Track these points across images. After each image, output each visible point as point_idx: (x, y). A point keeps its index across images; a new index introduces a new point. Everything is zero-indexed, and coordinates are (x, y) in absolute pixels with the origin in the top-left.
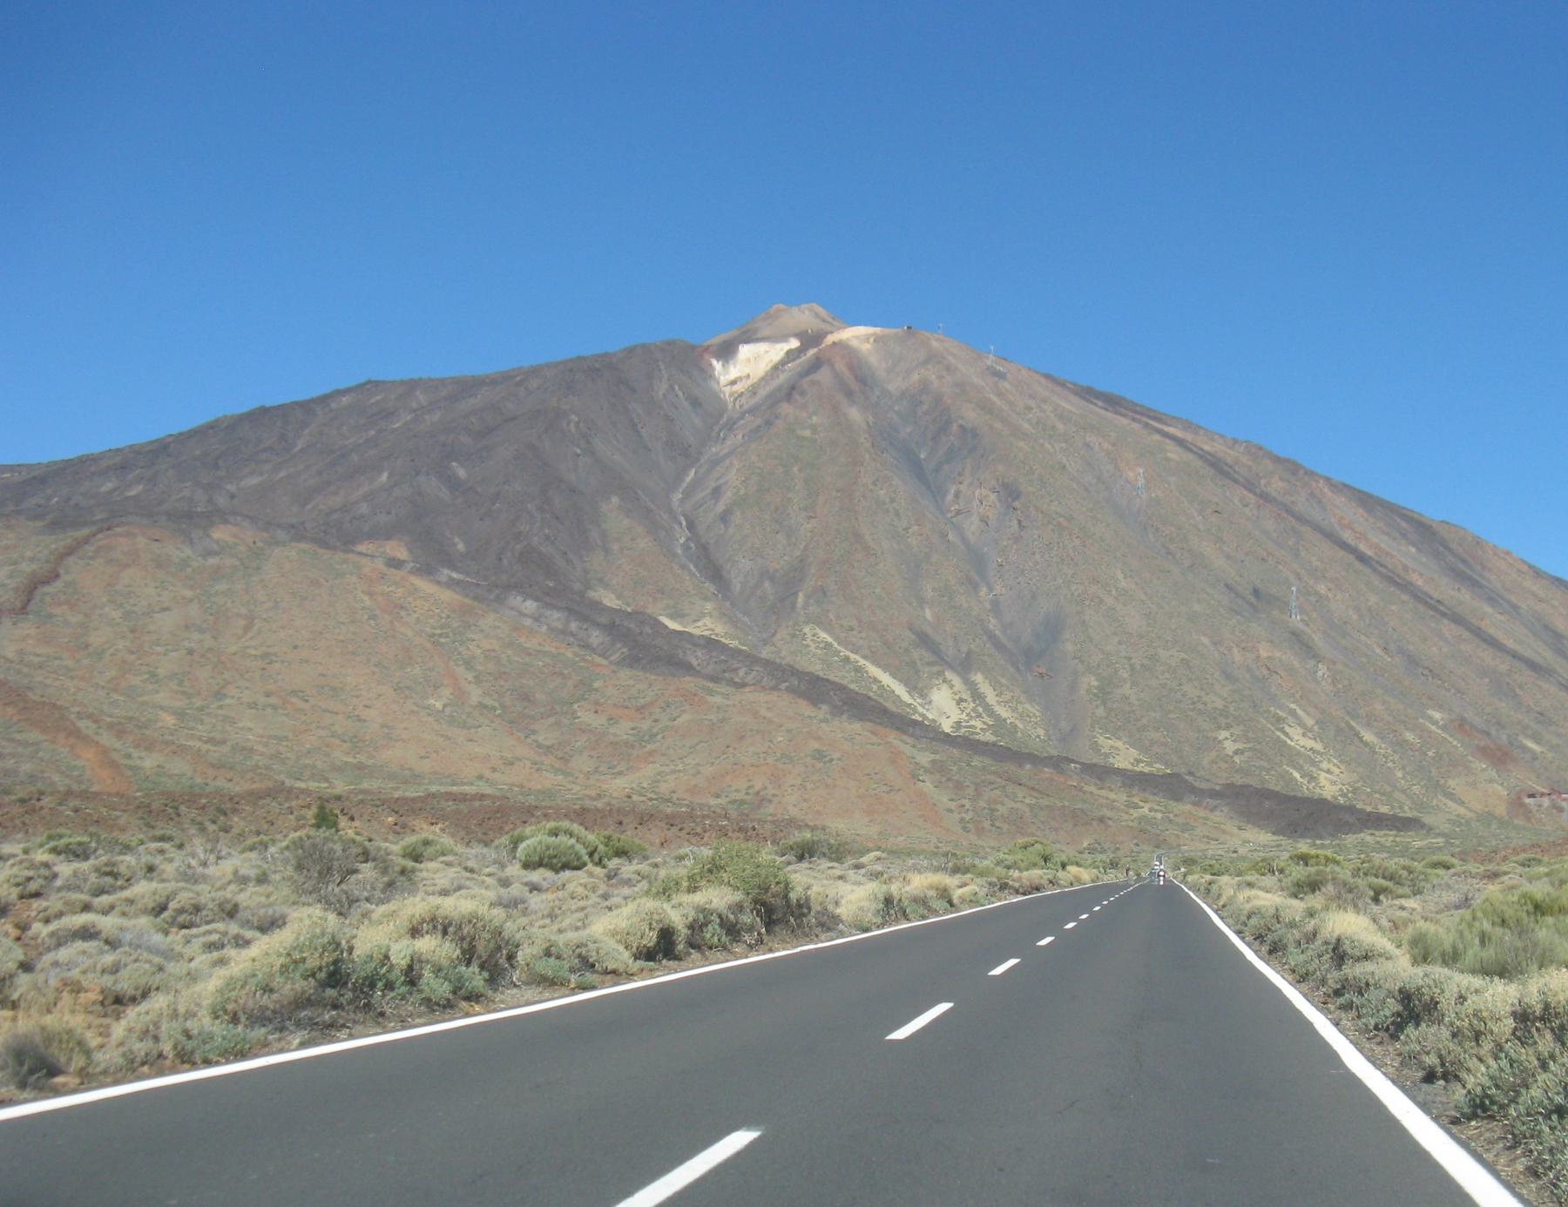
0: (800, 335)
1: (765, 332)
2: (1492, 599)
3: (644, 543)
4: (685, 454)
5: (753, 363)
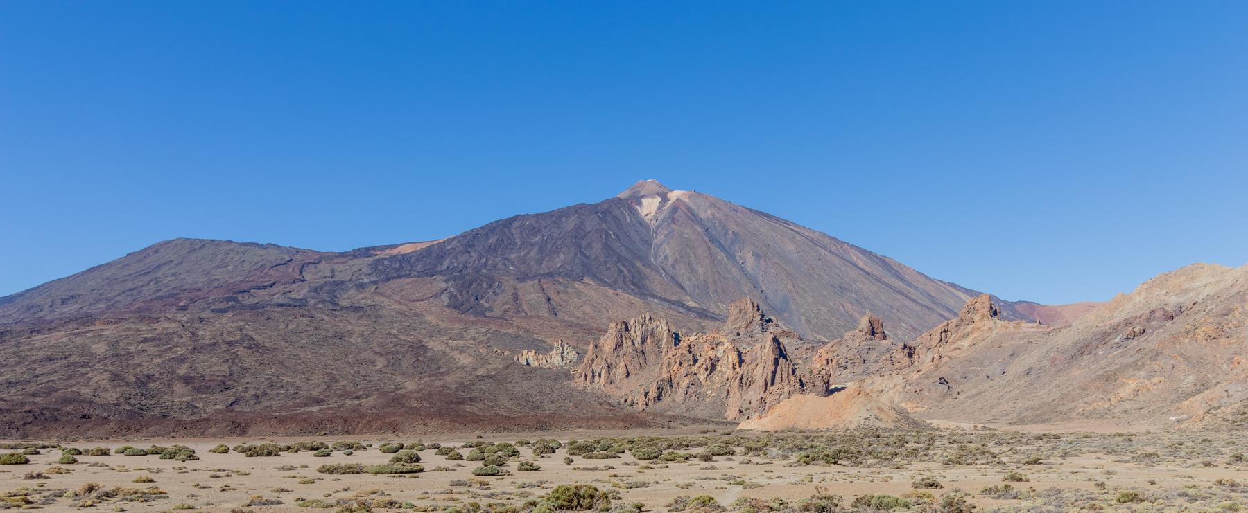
0: (658, 194)
1: (642, 193)
2: (910, 285)
3: (658, 277)
4: (647, 243)
5: (649, 207)
